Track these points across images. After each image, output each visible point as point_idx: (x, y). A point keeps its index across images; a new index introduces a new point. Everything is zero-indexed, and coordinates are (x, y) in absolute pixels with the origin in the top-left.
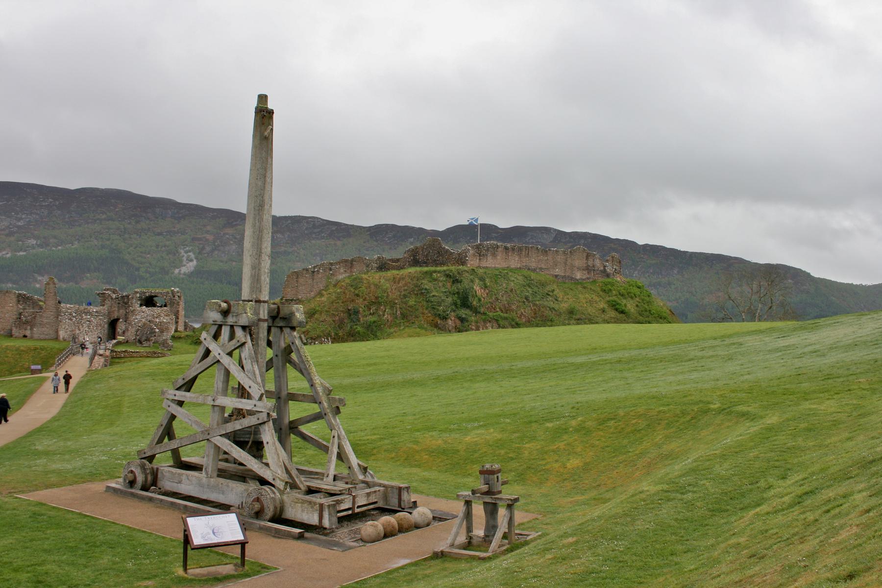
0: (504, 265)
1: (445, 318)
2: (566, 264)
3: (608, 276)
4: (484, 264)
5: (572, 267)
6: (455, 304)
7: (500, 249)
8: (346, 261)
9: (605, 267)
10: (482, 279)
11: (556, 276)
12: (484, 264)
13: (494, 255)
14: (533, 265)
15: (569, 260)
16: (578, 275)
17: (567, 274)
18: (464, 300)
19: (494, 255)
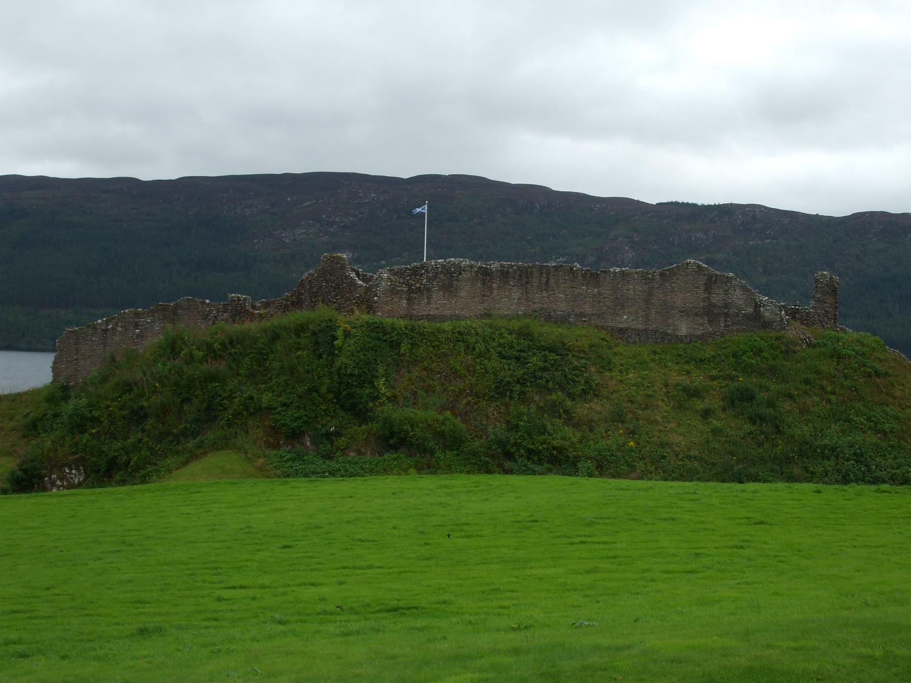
3: (766, 325)
13: (449, 288)
14: (562, 307)
16: (683, 328)
19: (449, 288)
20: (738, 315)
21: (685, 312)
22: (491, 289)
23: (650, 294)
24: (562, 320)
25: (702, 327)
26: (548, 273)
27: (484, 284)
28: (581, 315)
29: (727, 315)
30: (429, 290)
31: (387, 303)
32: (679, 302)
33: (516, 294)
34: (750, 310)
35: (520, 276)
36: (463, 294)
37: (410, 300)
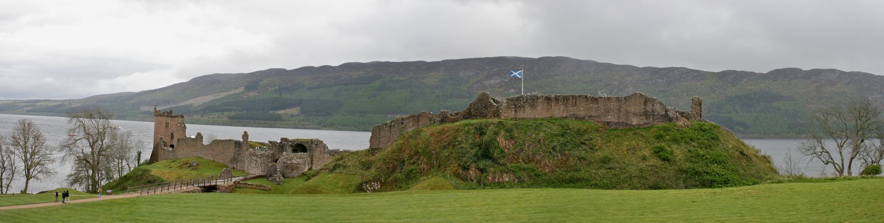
0: (547, 115)
1: (466, 169)
2: (619, 110)
3: (670, 120)
4: (521, 115)
5: (627, 113)
6: (476, 155)
7: (540, 100)
8: (414, 116)
9: (666, 111)
10: (509, 131)
11: (608, 123)
12: (521, 115)
13: (533, 106)
14: (582, 114)
15: (624, 107)
16: (635, 121)
17: (621, 121)
18: (486, 153)
19: (533, 106)
21: (635, 114)
24: (582, 119)
28: (591, 116)
32: (633, 110)
33: (562, 108)
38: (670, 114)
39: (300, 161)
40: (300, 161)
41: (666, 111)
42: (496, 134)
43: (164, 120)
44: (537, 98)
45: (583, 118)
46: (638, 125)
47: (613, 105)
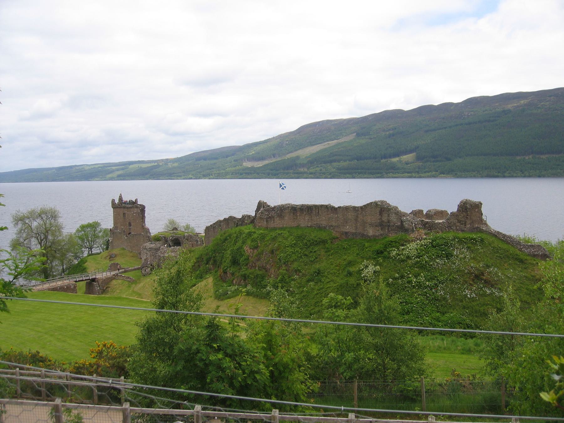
2: (356, 220)
3: (406, 231)
11: (346, 233)
14: (324, 223)
16: (371, 232)
20: (393, 226)
21: (371, 225)
22: (297, 216)
23: (357, 217)
25: (379, 232)
26: (318, 209)
27: (294, 214)
28: (332, 226)
29: (389, 226)
30: (273, 217)
31: (259, 223)
34: (399, 224)
35: (308, 210)
36: (286, 218)
37: (267, 221)
38: (406, 225)
39: (173, 254)
40: (173, 254)
41: (402, 222)
42: (244, 243)
43: (121, 211)
44: (285, 209)
45: (325, 228)
46: (374, 236)
47: (351, 215)
